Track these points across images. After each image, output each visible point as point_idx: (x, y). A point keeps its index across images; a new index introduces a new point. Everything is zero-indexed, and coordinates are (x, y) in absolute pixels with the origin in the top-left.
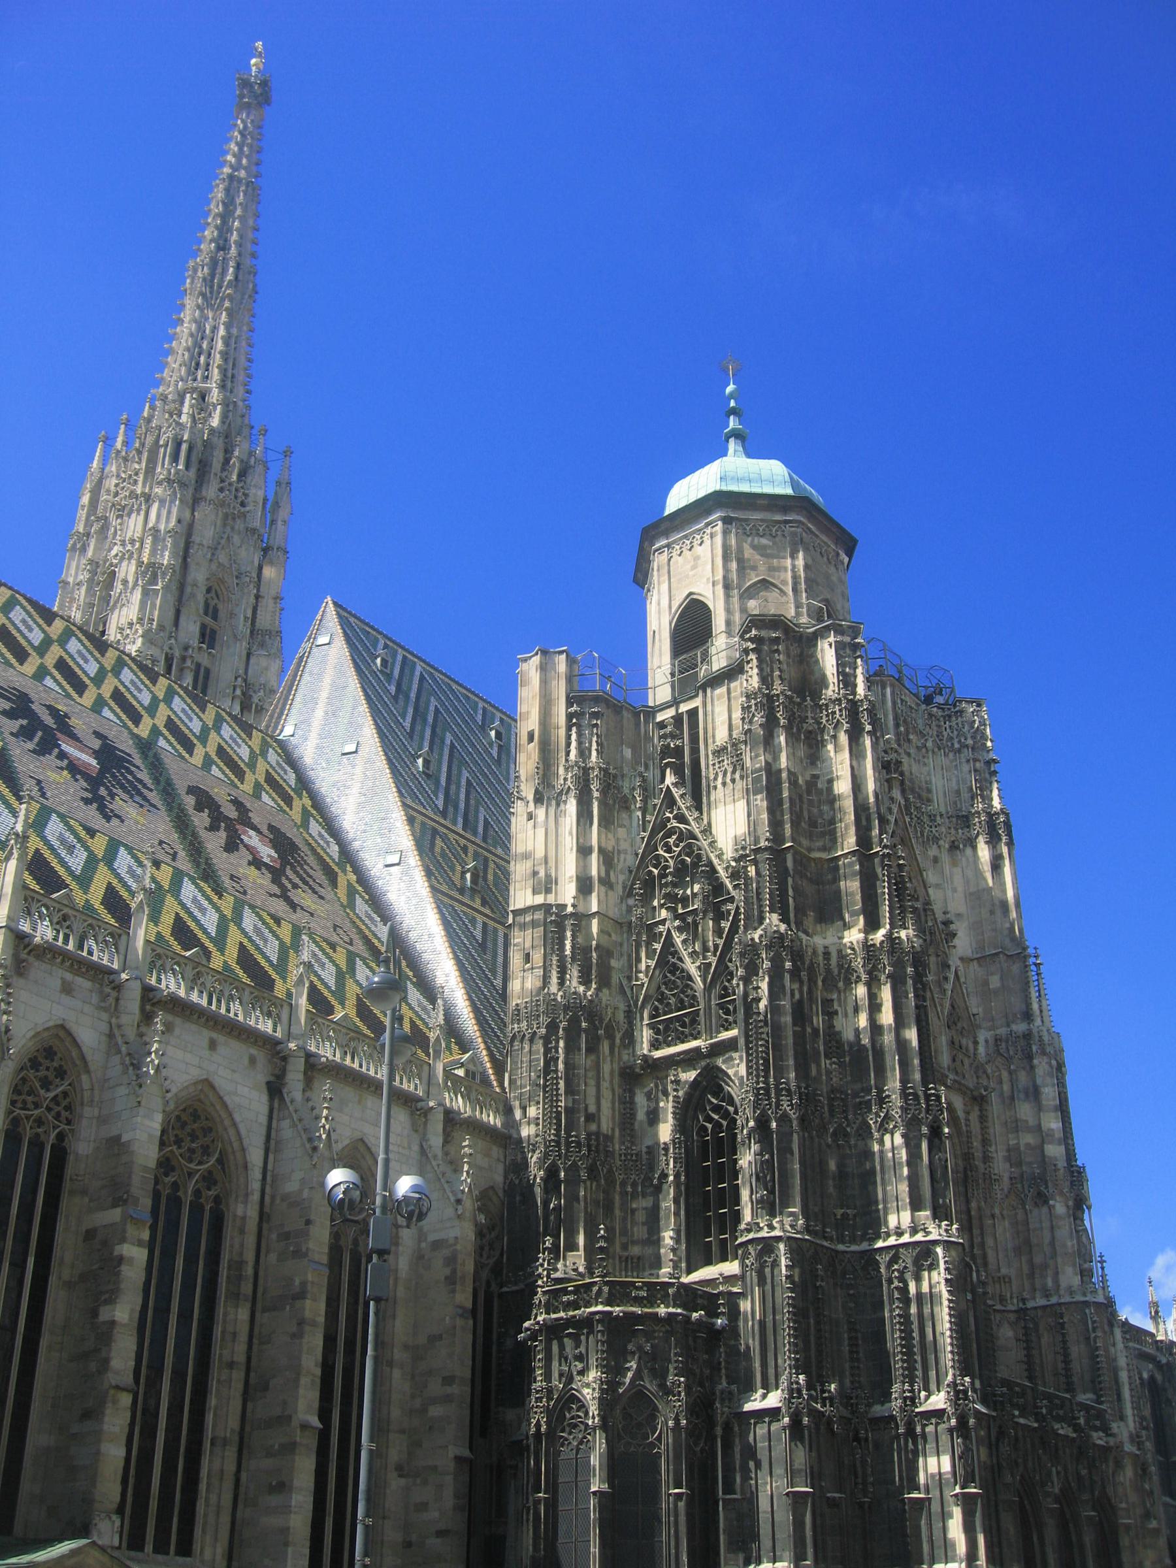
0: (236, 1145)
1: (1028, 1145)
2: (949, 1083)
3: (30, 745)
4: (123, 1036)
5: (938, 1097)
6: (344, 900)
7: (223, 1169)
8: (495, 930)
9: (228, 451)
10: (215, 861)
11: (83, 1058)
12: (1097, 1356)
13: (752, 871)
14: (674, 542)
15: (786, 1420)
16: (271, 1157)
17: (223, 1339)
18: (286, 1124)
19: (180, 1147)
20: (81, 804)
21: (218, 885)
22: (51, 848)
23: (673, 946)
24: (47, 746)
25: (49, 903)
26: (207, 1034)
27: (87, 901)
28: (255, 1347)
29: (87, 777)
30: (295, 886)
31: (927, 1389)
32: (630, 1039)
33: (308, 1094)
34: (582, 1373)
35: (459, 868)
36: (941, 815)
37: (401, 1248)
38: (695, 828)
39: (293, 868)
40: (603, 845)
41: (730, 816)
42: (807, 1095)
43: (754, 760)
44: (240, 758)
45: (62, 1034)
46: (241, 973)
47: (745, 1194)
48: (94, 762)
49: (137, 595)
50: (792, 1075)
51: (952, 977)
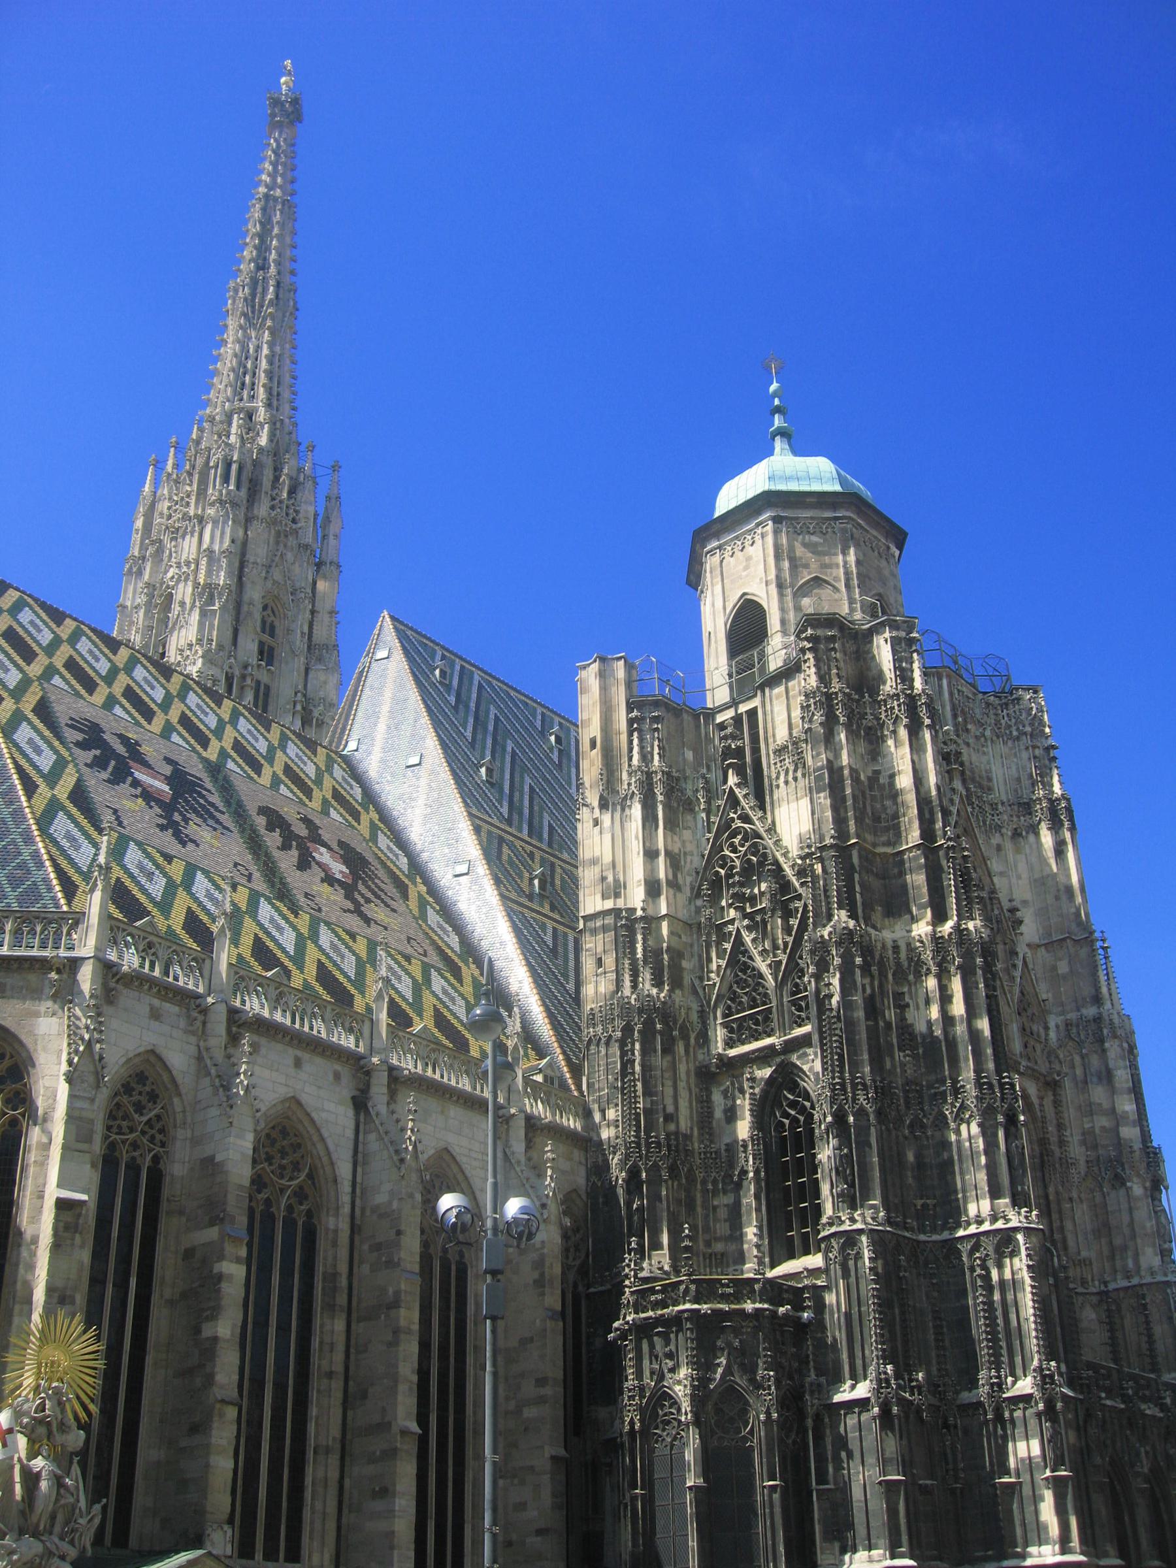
0: (325, 1159)
1: (1103, 1128)
2: (1022, 1069)
3: (105, 775)
4: (211, 1058)
5: (1013, 1086)
6: (416, 912)
7: (314, 1183)
8: (565, 935)
9: (277, 470)
10: (289, 880)
11: (173, 1080)
13: (818, 868)
14: (726, 543)
15: (876, 1410)
16: (359, 1170)
18: (372, 1137)
19: (271, 1164)
20: (157, 830)
21: (293, 904)
22: (131, 876)
23: (743, 945)
24: (120, 775)
25: (135, 931)
26: (292, 1052)
27: (169, 927)
28: (352, 1357)
29: (160, 803)
30: (368, 901)
31: (1013, 1374)
32: (704, 1039)
33: (392, 1106)
34: (673, 1370)
35: (527, 875)
36: (1003, 803)
38: (759, 827)
39: (365, 883)
40: (669, 848)
41: (794, 814)
42: (882, 1088)
43: (815, 758)
44: (307, 775)
45: (152, 1059)
46: (320, 990)
47: (825, 1189)
48: (166, 788)
49: (195, 617)
50: (867, 1069)
51: (1020, 964)
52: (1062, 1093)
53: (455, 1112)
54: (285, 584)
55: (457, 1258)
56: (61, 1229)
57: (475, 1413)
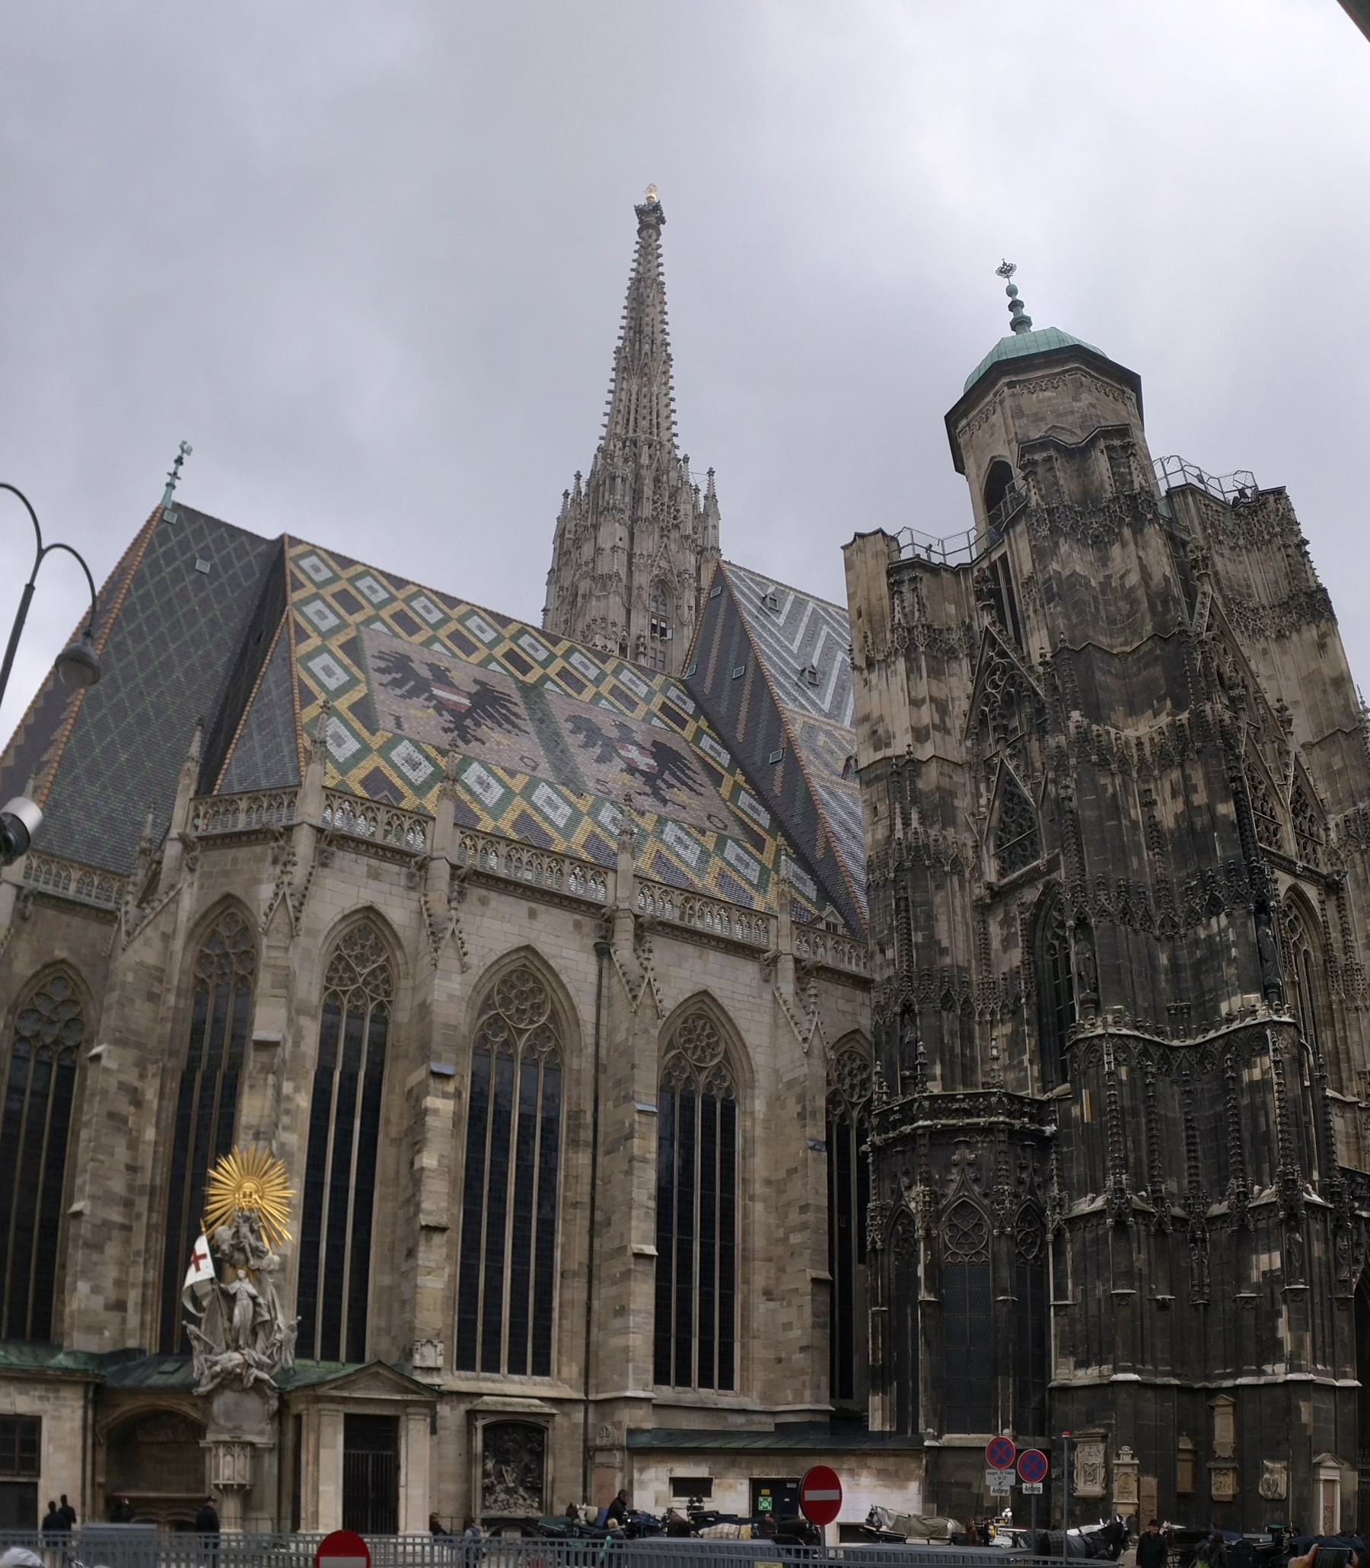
3: (399, 692)
6: (726, 794)
16: (604, 1013)
18: (615, 980)
20: (442, 733)
26: (525, 905)
28: (599, 1189)
30: (672, 786)
32: (977, 869)
37: (757, 1091)
40: (935, 694)
48: (467, 702)
51: (1292, 763)
53: (715, 959)
54: (671, 570)
57: (744, 1241)
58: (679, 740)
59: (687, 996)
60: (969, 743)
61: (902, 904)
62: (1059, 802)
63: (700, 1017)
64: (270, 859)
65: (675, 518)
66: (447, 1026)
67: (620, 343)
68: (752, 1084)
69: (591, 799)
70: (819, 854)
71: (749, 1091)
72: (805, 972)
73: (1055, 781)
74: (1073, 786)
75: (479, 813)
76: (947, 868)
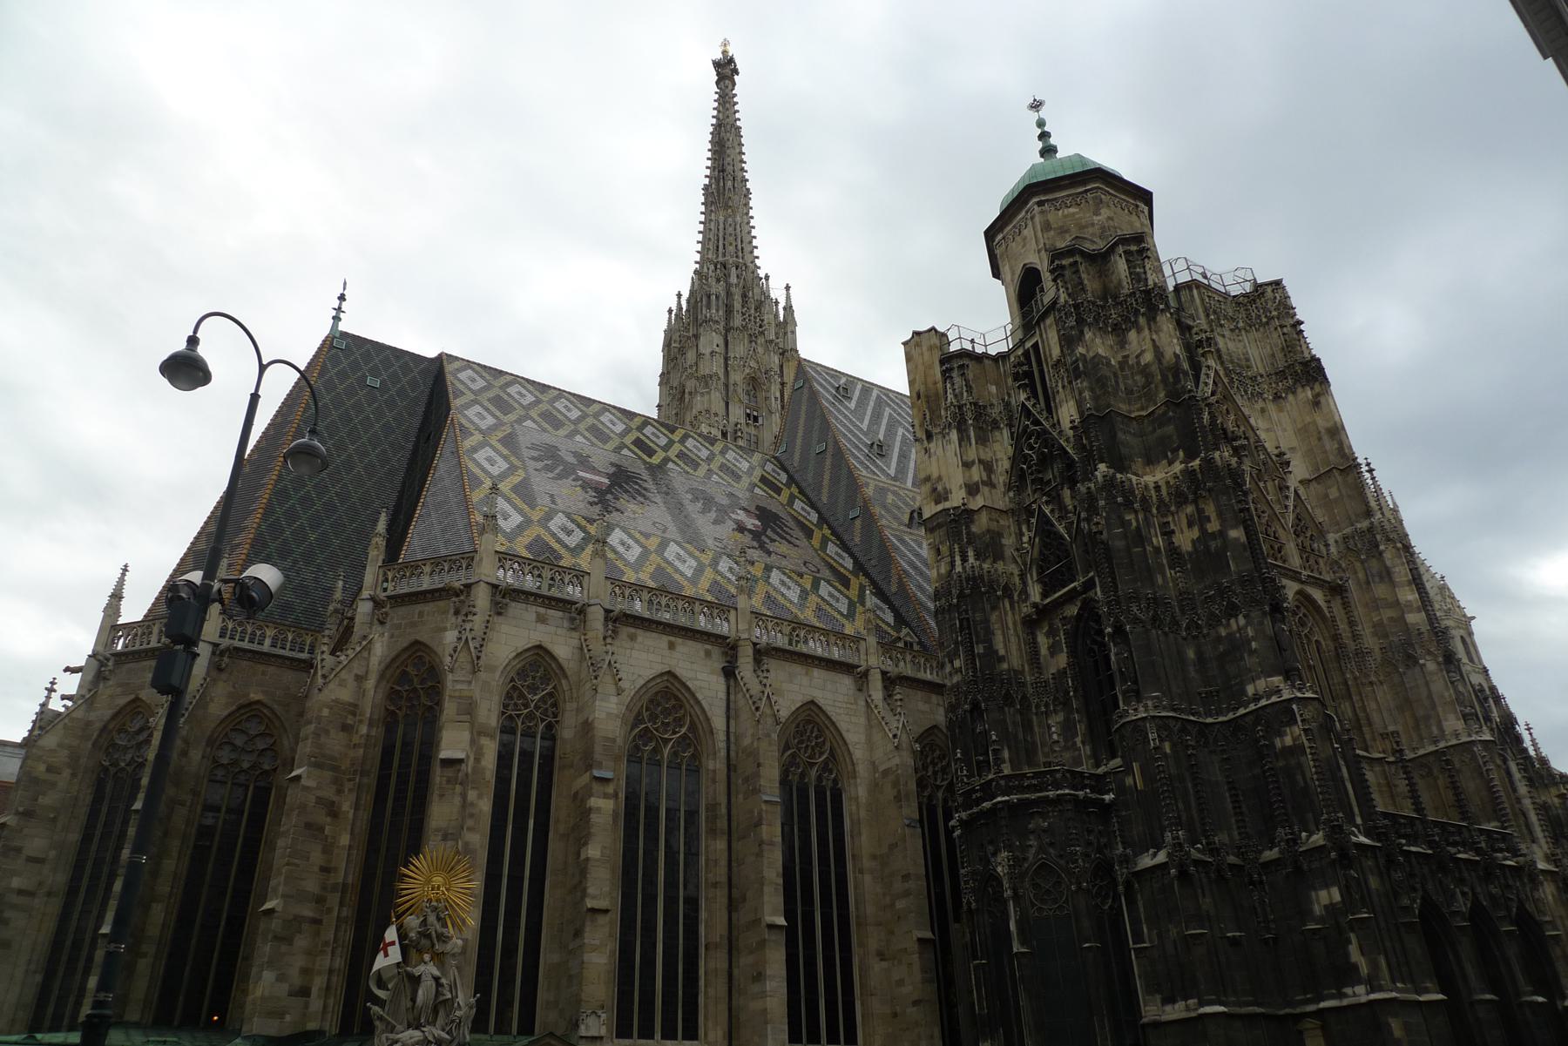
3: (550, 475)
12: (1493, 787)
16: (732, 722)
17: (707, 864)
18: (740, 696)
26: (665, 639)
28: (735, 869)
30: (775, 541)
32: (1024, 593)
34: (995, 854)
36: (1262, 376)
37: (859, 781)
39: (774, 531)
40: (982, 457)
45: (541, 653)
48: (607, 481)
52: (1349, 595)
53: (817, 673)
55: (830, 784)
56: (444, 782)
57: (857, 909)
58: (776, 504)
59: (798, 705)
60: (1011, 494)
61: (965, 623)
62: (1093, 536)
63: (809, 722)
64: (452, 611)
65: (761, 326)
66: (607, 739)
67: (707, 181)
68: (854, 775)
69: (711, 554)
70: (894, 588)
71: (852, 781)
72: (889, 681)
73: (1088, 520)
74: (1103, 522)
75: (623, 568)
76: (999, 593)
